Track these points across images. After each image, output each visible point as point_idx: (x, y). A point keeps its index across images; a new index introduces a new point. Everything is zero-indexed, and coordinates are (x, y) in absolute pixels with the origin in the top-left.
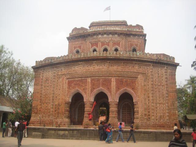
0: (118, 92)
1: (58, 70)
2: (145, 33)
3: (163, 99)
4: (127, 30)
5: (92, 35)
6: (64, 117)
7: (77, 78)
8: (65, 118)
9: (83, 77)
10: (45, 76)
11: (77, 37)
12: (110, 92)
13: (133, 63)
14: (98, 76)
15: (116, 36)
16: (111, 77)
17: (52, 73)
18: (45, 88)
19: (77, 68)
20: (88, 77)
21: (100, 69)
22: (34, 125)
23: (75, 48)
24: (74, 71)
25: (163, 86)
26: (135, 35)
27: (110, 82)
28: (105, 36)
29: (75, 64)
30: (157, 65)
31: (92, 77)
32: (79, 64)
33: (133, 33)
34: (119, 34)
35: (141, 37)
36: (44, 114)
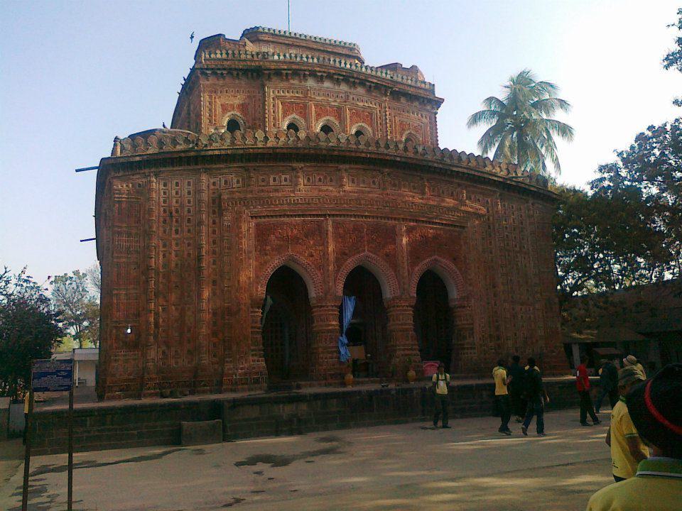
0: (417, 269)
1: (212, 181)
2: (438, 94)
3: (527, 290)
4: (389, 77)
5: (287, 74)
6: (253, 355)
7: (288, 216)
8: (256, 358)
9: (306, 216)
10: (162, 200)
11: (235, 73)
12: (395, 266)
13: (452, 183)
14: (355, 216)
15: (360, 90)
16: (395, 219)
17: (189, 193)
18: (164, 246)
19: (286, 180)
20: (325, 216)
21: (363, 192)
22: (130, 396)
23: (225, 109)
24: (277, 191)
25: (525, 253)
26: (412, 98)
27: (392, 235)
28: (327, 84)
29: (281, 168)
30: (513, 194)
31: (337, 215)
32: (293, 169)
33: (411, 91)
34: (370, 87)
35: (428, 108)
36: (168, 347)
